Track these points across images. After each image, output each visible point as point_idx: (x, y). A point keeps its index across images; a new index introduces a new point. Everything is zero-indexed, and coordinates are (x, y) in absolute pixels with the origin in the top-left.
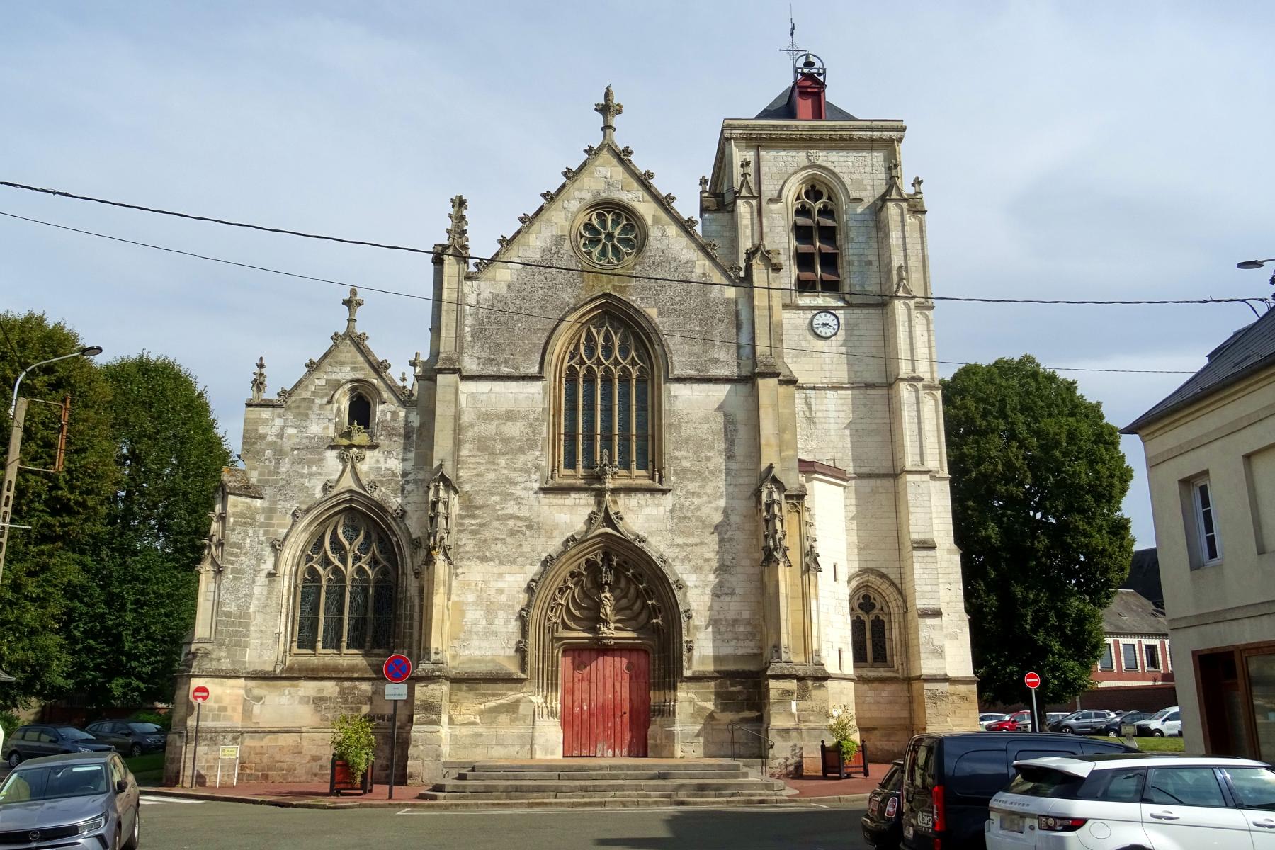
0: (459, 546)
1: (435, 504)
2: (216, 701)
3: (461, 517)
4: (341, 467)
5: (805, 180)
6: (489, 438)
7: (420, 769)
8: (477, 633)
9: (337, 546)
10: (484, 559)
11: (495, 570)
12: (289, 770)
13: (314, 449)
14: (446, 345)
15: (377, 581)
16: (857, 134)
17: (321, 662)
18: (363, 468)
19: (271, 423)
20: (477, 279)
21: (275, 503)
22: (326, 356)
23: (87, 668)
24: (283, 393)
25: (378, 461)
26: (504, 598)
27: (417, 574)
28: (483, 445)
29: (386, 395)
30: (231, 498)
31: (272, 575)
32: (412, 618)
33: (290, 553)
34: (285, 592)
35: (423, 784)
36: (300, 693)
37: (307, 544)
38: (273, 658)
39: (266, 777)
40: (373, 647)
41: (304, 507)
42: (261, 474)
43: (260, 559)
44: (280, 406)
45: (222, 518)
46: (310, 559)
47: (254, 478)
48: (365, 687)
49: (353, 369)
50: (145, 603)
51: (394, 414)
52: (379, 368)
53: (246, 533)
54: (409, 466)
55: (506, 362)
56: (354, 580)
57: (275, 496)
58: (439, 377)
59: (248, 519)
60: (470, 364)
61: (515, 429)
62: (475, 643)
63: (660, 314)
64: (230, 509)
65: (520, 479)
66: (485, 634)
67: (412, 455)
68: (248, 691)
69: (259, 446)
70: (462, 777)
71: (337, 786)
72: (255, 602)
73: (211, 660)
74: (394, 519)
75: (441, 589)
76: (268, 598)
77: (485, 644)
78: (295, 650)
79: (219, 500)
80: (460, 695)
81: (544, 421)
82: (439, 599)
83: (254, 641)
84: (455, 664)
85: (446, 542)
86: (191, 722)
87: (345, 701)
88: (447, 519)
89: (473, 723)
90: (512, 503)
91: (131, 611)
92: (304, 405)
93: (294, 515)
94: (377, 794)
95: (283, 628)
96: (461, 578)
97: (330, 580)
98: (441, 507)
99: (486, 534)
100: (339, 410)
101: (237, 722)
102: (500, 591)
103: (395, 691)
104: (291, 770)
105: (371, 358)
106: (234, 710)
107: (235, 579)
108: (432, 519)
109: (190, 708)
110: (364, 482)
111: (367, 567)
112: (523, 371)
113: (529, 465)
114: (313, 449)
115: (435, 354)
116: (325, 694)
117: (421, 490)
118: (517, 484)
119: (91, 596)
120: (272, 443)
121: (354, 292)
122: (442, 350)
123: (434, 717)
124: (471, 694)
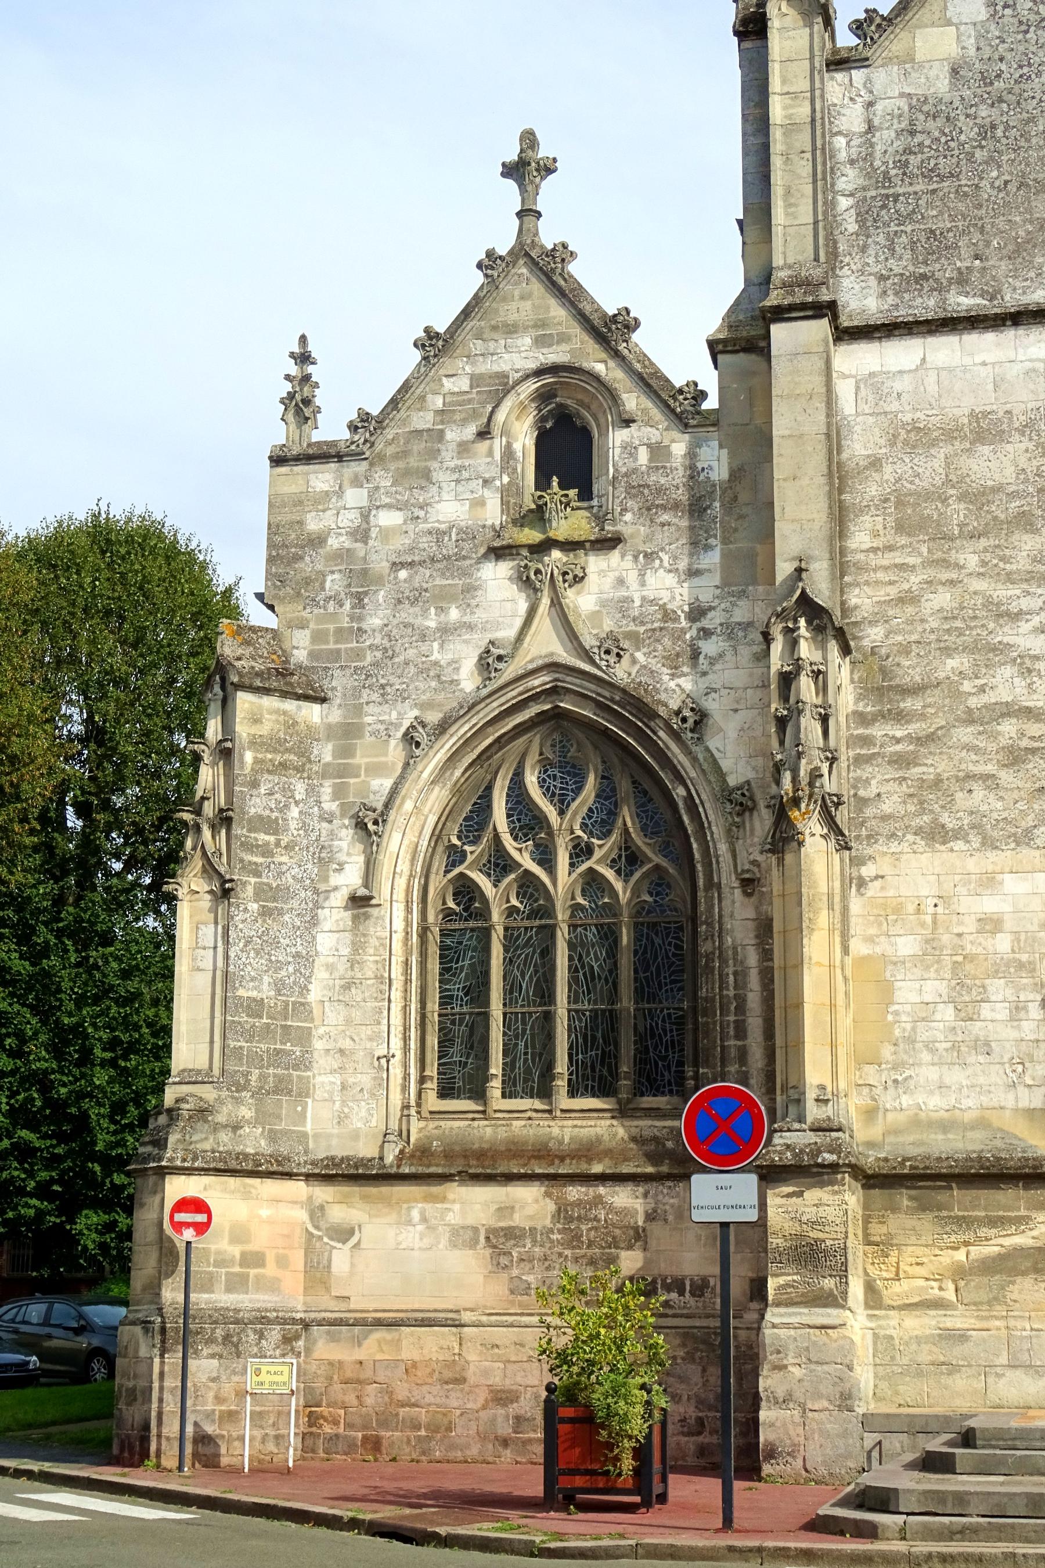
0: (863, 802)
1: (787, 680)
2: (234, 1240)
3: (861, 718)
4: (523, 606)
6: (927, 496)
7: (797, 1433)
8: (930, 1046)
9: (528, 821)
10: (937, 835)
11: (972, 864)
12: (433, 1428)
13: (450, 560)
14: (791, 247)
15: (640, 910)
17: (502, 1133)
18: (583, 601)
19: (338, 503)
20: (863, 62)
21: (358, 710)
22: (466, 313)
23: (22, 1192)
24: (362, 423)
25: (621, 582)
26: (1003, 943)
27: (749, 884)
28: (911, 515)
29: (632, 401)
30: (244, 701)
31: (360, 902)
32: (741, 1008)
33: (406, 839)
34: (397, 947)
35: (809, 1477)
36: (455, 1217)
37: (447, 816)
38: (377, 1122)
39: (374, 1444)
40: (639, 1091)
41: (433, 717)
42: (318, 637)
43: (326, 860)
44: (357, 456)
45: (225, 753)
46: (456, 856)
47: (300, 648)
48: (626, 1199)
49: (540, 342)
50: (132, 1048)
51: (658, 451)
52: (611, 331)
53: (288, 791)
54: (707, 589)
55: (962, 280)
56: (576, 908)
57: (356, 692)
58: (777, 331)
59: (291, 754)
60: (860, 297)
62: (929, 1074)
64: (242, 729)
65: (1025, 604)
66: (955, 1047)
67: (712, 559)
68: (317, 1212)
69: (307, 566)
70: (934, 1463)
71: (565, 1482)
72: (320, 974)
73: (216, 1128)
74: (676, 735)
75: (823, 919)
76: (352, 963)
77: (956, 1076)
78: (432, 1101)
79: (215, 708)
80: (895, 1223)
82: (817, 947)
83: (323, 1078)
84: (875, 1132)
85: (829, 785)
86: (171, 1294)
87: (574, 1239)
88: (824, 719)
89: (938, 1304)
90: (1008, 671)
91: (103, 1064)
92: (417, 446)
93: (410, 739)
94: (685, 1507)
95: (396, 1043)
96: (873, 889)
97: (512, 911)
98: (806, 687)
99: (936, 765)
100: (508, 453)
101: (292, 1296)
102: (991, 925)
103: (721, 1195)
104: (440, 1427)
105: (587, 308)
106: (282, 1262)
107: (265, 913)
108: (782, 723)
109: (168, 1255)
110: (589, 641)
111: (609, 874)
112: (1012, 299)
114: (449, 563)
115: (760, 278)
116: (518, 1220)
117: (746, 653)
118: (1017, 616)
119: (20, 1036)
120: (343, 555)
121: (529, 139)
122: (778, 261)
123: (829, 1283)
124: (925, 1223)
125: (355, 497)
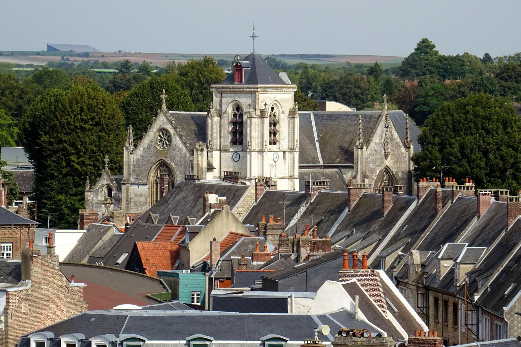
5: (233, 105)
16: (245, 90)
49: (107, 181)
55: (140, 179)
61: (142, 199)
120: (91, 202)
125: (92, 196)
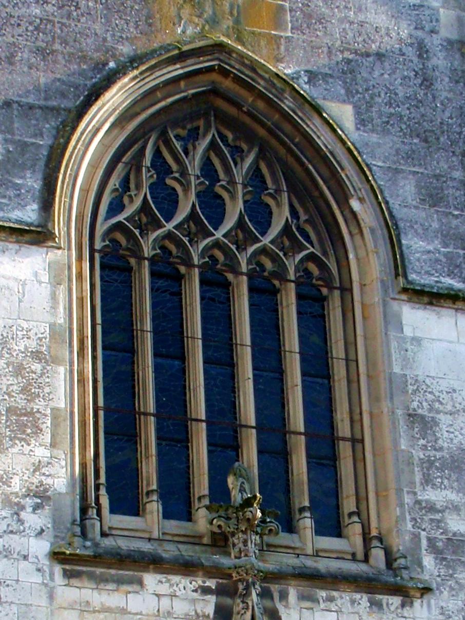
63: (362, 122)
81: (56, 361)
113: (16, 485)
